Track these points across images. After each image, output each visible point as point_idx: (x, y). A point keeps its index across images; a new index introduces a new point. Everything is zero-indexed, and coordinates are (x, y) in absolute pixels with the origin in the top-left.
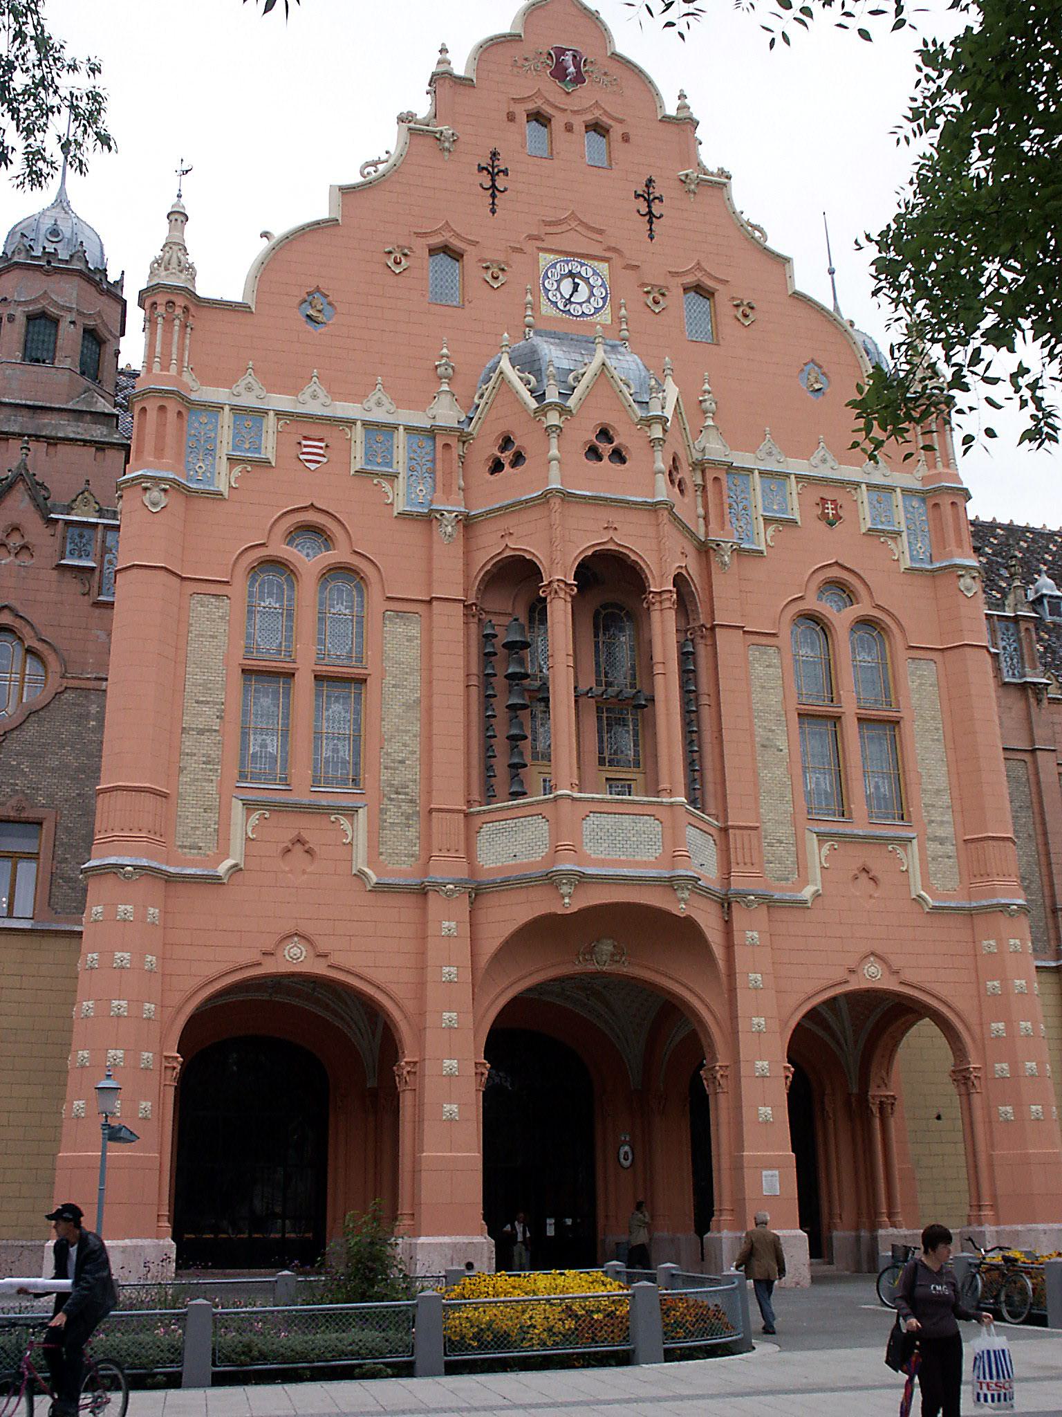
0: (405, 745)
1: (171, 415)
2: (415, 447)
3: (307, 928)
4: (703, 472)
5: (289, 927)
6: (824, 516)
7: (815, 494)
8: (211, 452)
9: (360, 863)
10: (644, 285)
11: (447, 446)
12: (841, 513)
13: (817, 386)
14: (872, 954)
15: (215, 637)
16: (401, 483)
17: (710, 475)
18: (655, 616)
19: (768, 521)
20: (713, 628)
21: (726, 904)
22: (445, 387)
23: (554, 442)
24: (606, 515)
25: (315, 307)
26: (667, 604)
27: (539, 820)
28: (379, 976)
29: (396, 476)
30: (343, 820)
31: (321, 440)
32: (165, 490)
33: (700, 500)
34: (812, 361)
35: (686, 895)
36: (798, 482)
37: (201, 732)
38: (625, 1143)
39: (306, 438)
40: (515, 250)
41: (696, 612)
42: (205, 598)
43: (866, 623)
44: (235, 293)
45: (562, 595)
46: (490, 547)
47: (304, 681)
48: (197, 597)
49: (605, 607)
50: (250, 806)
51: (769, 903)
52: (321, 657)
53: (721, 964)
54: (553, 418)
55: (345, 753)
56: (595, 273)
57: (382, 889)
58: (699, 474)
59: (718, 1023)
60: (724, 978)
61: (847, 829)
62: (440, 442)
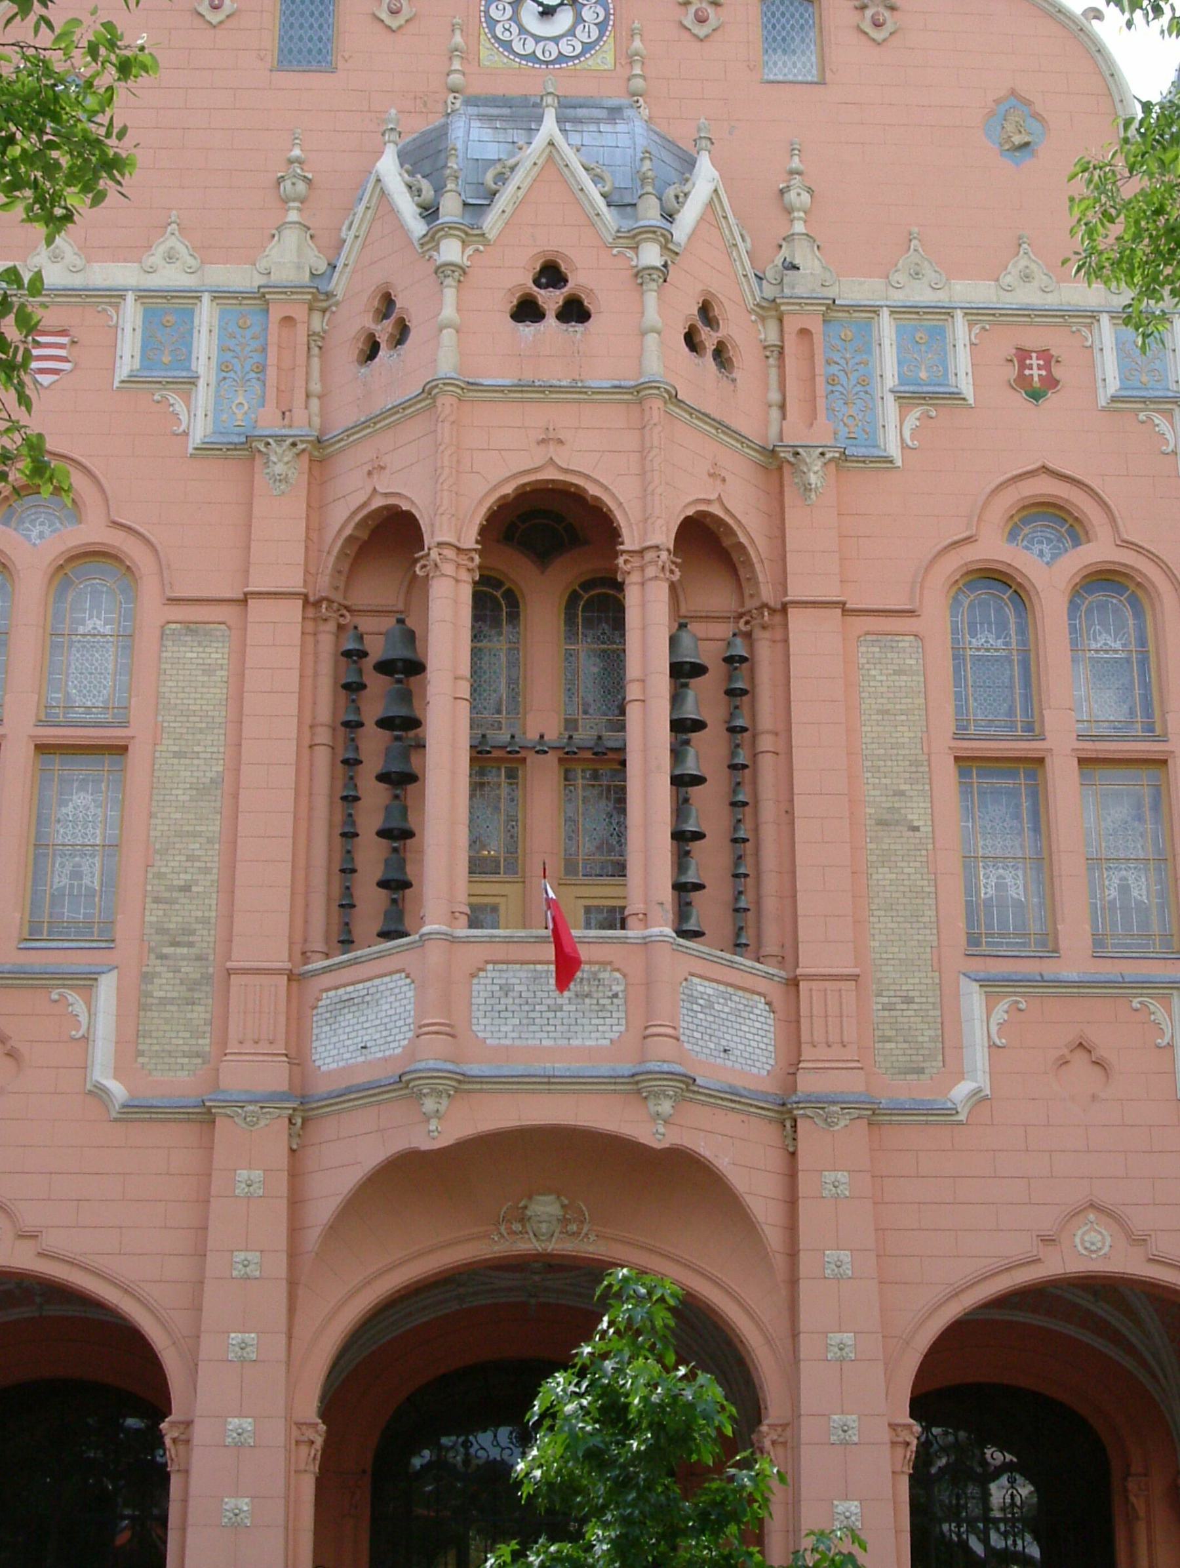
0: (191, 858)
4: (781, 321)
6: (1023, 382)
7: (1005, 343)
9: (103, 1073)
11: (288, 320)
12: (1057, 372)
13: (1017, 139)
14: (1092, 1206)
16: (203, 396)
17: (792, 325)
18: (632, 598)
20: (784, 609)
21: (785, 1114)
22: (293, 216)
23: (450, 295)
24: (538, 416)
26: (651, 571)
27: (400, 981)
29: (193, 381)
30: (72, 996)
31: (63, 333)
33: (773, 372)
34: (1013, 92)
35: (666, 1107)
36: (971, 324)
41: (753, 579)
43: (1105, 580)
45: (448, 568)
49: (587, 585)
51: (875, 1115)
53: (774, 1237)
54: (451, 251)
57: (137, 1112)
58: (772, 325)
60: (780, 1262)
61: (1050, 969)
62: (276, 313)
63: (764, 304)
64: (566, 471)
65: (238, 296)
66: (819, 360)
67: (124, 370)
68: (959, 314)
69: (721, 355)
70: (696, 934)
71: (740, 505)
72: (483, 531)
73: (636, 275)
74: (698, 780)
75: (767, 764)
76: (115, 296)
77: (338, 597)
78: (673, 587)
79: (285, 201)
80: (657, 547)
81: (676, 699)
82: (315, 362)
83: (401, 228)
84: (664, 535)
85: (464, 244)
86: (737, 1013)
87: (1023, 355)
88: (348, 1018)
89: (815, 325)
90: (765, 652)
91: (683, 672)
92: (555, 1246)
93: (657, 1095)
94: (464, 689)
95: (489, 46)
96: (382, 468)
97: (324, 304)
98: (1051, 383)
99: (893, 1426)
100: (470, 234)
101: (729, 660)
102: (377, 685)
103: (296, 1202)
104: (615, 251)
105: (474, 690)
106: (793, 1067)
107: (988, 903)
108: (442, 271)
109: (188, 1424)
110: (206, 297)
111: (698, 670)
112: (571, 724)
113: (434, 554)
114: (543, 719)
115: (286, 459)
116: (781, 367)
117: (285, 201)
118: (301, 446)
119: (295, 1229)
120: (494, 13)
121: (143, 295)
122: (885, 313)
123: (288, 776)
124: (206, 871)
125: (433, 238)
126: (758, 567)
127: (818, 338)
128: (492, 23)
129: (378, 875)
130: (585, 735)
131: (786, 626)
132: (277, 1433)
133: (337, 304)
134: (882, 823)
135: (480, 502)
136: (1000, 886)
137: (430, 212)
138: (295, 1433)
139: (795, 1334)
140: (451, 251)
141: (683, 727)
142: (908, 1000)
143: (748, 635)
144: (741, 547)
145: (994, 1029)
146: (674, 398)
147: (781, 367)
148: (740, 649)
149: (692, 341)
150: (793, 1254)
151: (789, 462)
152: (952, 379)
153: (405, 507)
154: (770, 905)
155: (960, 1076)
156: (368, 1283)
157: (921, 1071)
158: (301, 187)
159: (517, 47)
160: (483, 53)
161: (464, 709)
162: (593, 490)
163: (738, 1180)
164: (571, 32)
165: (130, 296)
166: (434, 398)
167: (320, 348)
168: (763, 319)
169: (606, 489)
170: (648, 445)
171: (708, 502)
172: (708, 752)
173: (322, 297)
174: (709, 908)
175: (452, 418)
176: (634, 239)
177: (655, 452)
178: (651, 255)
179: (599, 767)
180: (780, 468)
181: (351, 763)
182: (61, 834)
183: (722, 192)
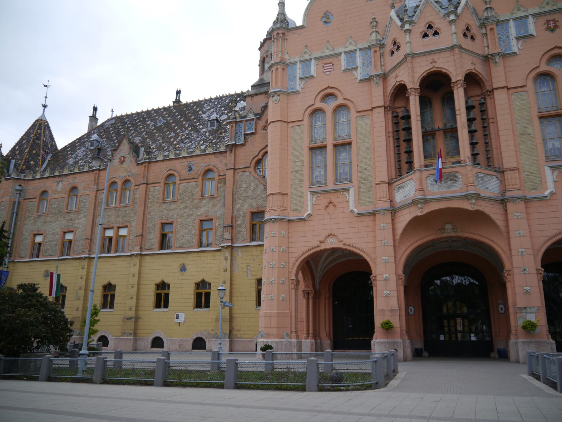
0: (366, 163)
1: (280, 70)
2: (364, 55)
3: (334, 232)
4: (486, 28)
5: (328, 232)
8: (295, 77)
9: (352, 207)
12: (558, 24)
15: (301, 138)
16: (359, 70)
17: (488, 28)
18: (455, 92)
19: (518, 39)
20: (493, 90)
21: (503, 202)
22: (374, 30)
23: (408, 36)
24: (430, 58)
25: (326, 19)
26: (459, 85)
27: (411, 181)
28: (360, 246)
29: (357, 68)
30: (345, 193)
32: (279, 95)
33: (485, 40)
35: (473, 201)
36: (534, 18)
37: (297, 172)
38: (501, 304)
39: (325, 64)
41: (484, 86)
42: (296, 127)
44: (299, 22)
45: (413, 93)
46: (392, 83)
47: (330, 148)
48: (293, 128)
50: (313, 193)
51: (526, 200)
52: (335, 138)
53: (503, 229)
54: (407, 27)
55: (347, 170)
57: (360, 215)
59: (504, 252)
65: (365, 49)
66: (496, 34)
67: (343, 69)
68: (530, 17)
69: (472, 38)
70: (479, 164)
71: (479, 68)
72: (421, 84)
74: (475, 131)
75: (492, 126)
76: (340, 54)
77: (392, 105)
78: (465, 89)
79: (373, 27)
80: (460, 80)
81: (468, 114)
82: (382, 59)
83: (397, 25)
84: (461, 77)
85: (410, 25)
86: (489, 180)
87: (548, 22)
88: (401, 190)
89: (494, 26)
90: (488, 101)
91: (469, 108)
92: (452, 234)
93: (471, 199)
94: (419, 118)
98: (556, 27)
99: (537, 270)
100: (411, 23)
101: (480, 104)
102: (402, 122)
103: (394, 230)
105: (421, 118)
106: (504, 191)
107: (550, 150)
108: (406, 31)
109: (376, 276)
110: (358, 50)
111: (473, 107)
112: (445, 124)
113: (409, 91)
114: (439, 124)
116: (487, 38)
117: (373, 27)
119: (394, 235)
121: (346, 53)
122: (511, 20)
123: (384, 143)
124: (370, 165)
126: (486, 83)
127: (495, 30)
129: (406, 161)
130: (448, 126)
131: (493, 94)
132: (394, 277)
134: (521, 134)
136: (553, 145)
137: (401, 20)
138: (398, 277)
139: (510, 250)
140: (407, 27)
141: (470, 121)
142: (532, 173)
143: (485, 99)
144: (481, 79)
145: (555, 177)
146: (461, 47)
147: (487, 38)
148: (483, 101)
149: (465, 35)
150: (508, 232)
152: (530, 31)
153: (403, 83)
154: (495, 156)
155: (547, 189)
156: (411, 245)
157: (537, 189)
158: (375, 23)
161: (419, 123)
162: (444, 71)
163: (493, 216)
165: (343, 53)
168: (482, 28)
171: (472, 69)
172: (477, 125)
174: (481, 158)
176: (448, 15)
178: (452, 17)
179: (451, 132)
181: (398, 139)
182: (341, 162)
183: (469, 2)
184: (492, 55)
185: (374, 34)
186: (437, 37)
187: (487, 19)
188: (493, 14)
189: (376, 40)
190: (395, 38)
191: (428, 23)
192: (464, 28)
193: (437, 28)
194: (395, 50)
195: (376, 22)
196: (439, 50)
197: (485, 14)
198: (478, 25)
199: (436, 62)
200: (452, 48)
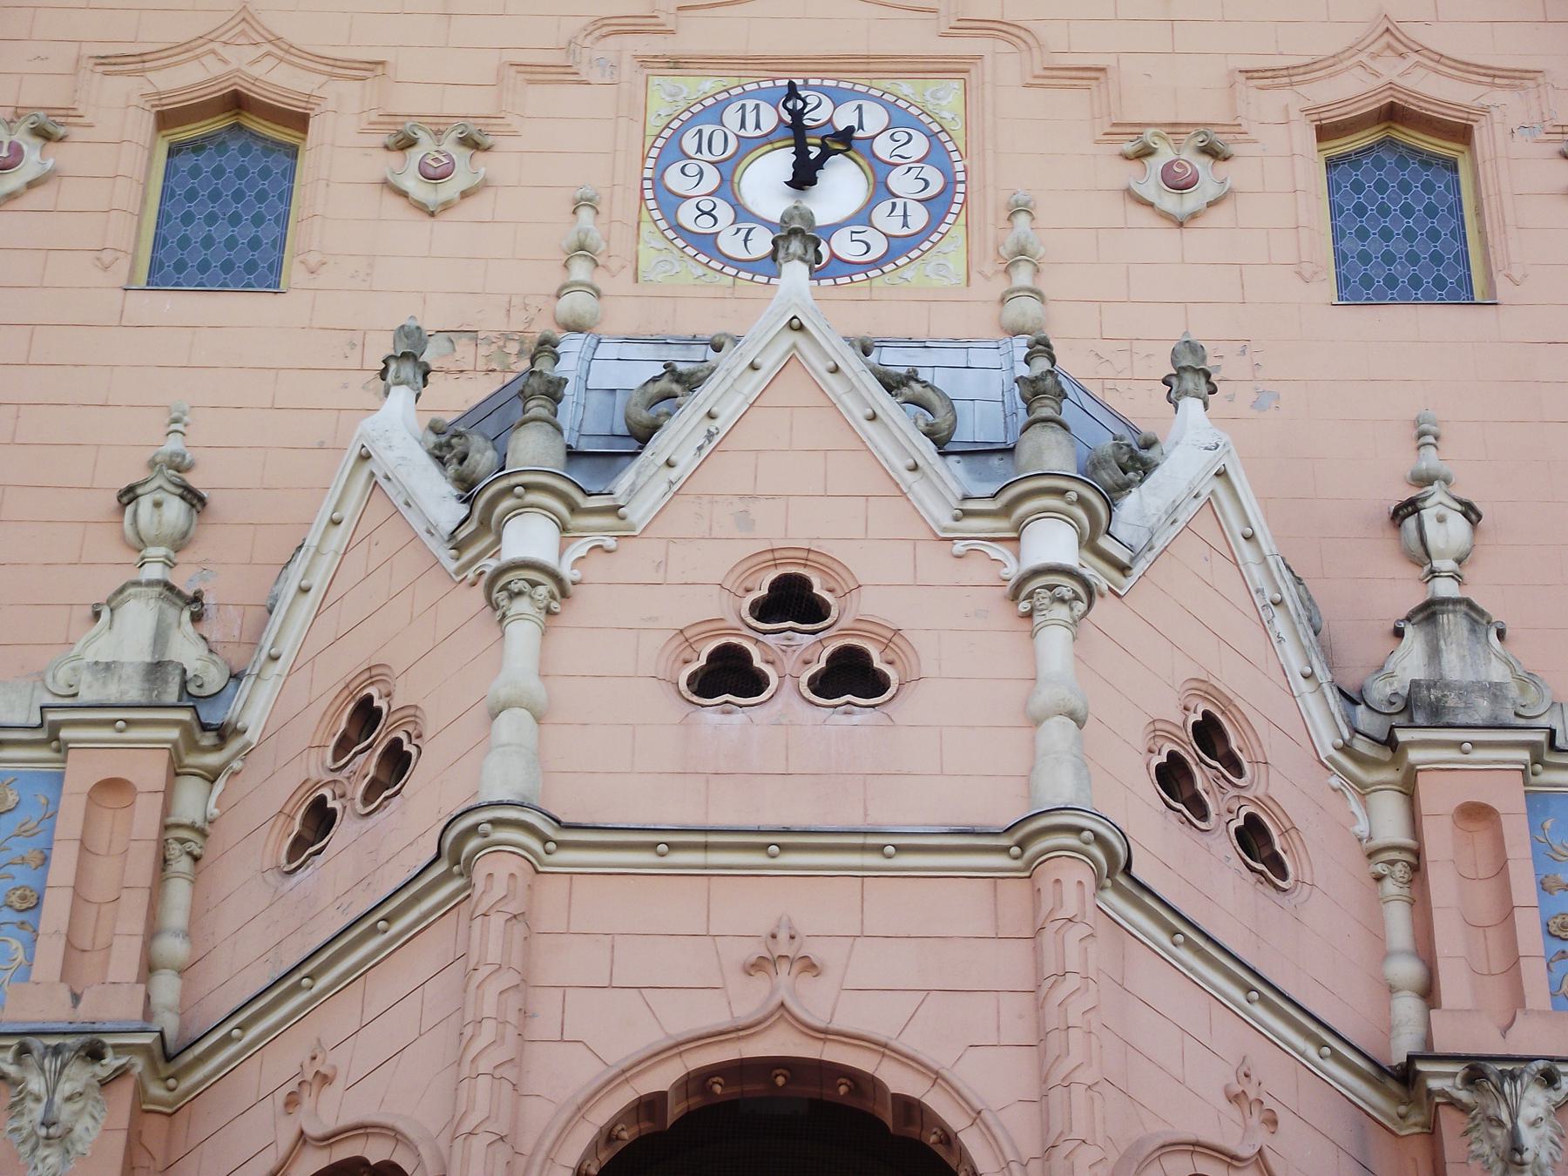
4: (1409, 792)
10: (1119, 129)
17: (1439, 797)
22: (154, 572)
24: (751, 907)
33: (1398, 920)
40: (535, 73)
56: (899, 118)
62: (82, 773)
63: (1361, 745)
64: (824, 1034)
73: (1015, 596)
82: (179, 892)
95: (663, 244)
96: (325, 1079)
97: (213, 759)
104: (959, 547)
108: (501, 587)
115: (66, 1088)
116: (1420, 904)
117: (140, 543)
118: (111, 1062)
120: (673, 179)
125: (484, 524)
127: (1516, 830)
128: (669, 201)
133: (246, 752)
135: (581, 1111)
140: (529, 537)
147: (1420, 904)
151: (1453, 1103)
158: (175, 509)
159: (730, 244)
160: (647, 257)
162: (898, 1080)
164: (863, 217)
166: (467, 872)
167: (196, 859)
169: (937, 1077)
170: (1050, 968)
173: (208, 739)
175: (513, 908)
177: (1072, 982)
178: (1053, 542)
180: (1432, 1131)
184: (1476, 1070)
185: (140, 616)
186: (850, 719)
187: (1423, 706)
188: (1497, 672)
189: (156, 669)
190: (373, 673)
191: (773, 556)
192: (1180, 717)
193: (864, 625)
194: (347, 796)
195: (194, 499)
196: (865, 839)
197: (1410, 663)
198: (1327, 741)
199: (810, 966)
200: (1026, 838)
